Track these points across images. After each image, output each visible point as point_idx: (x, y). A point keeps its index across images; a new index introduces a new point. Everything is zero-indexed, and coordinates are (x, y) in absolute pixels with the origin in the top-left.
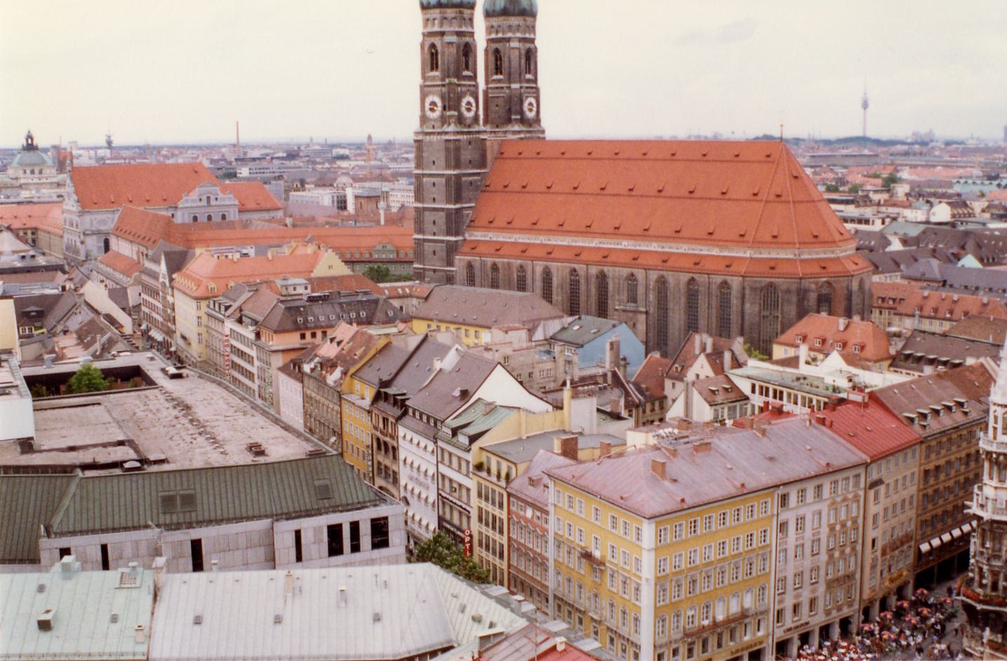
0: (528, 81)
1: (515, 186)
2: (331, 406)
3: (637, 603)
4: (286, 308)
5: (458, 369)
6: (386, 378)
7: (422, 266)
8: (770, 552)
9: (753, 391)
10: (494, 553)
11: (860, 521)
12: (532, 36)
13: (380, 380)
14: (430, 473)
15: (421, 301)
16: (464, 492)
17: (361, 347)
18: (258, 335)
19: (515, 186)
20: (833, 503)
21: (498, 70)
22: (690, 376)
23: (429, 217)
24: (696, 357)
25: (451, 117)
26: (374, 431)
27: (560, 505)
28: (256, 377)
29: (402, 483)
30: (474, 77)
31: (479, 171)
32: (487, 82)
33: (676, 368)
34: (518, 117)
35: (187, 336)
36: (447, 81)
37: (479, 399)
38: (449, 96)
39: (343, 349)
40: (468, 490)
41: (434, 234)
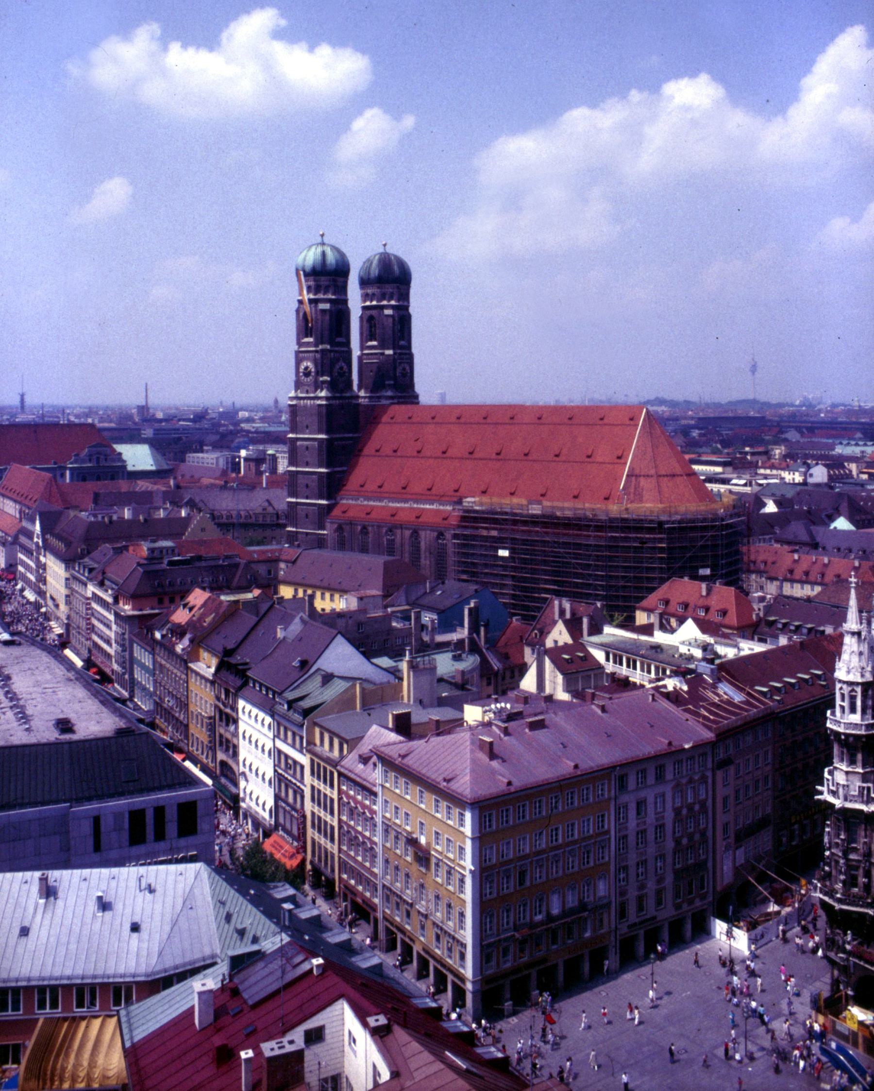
0: (402, 347)
1: (387, 450)
2: (179, 674)
3: (462, 896)
4: (144, 572)
5: (300, 639)
6: (230, 646)
7: (294, 529)
8: (609, 839)
9: (608, 659)
10: (326, 836)
11: (709, 803)
12: (406, 303)
13: (225, 648)
14: (267, 749)
15: (289, 565)
16: (298, 768)
17: (211, 614)
18: (116, 600)
19: (387, 450)
20: (678, 785)
21: (372, 337)
22: (549, 643)
23: (301, 480)
24: (555, 623)
25: (323, 382)
26: (217, 702)
27: (387, 785)
28: (113, 642)
29: (241, 759)
30: (348, 343)
31: (351, 435)
32: (362, 348)
33: (536, 634)
34: (392, 382)
35: (55, 597)
36: (320, 347)
37: (319, 669)
38: (322, 362)
39: (194, 616)
40: (302, 767)
41: (307, 498)
